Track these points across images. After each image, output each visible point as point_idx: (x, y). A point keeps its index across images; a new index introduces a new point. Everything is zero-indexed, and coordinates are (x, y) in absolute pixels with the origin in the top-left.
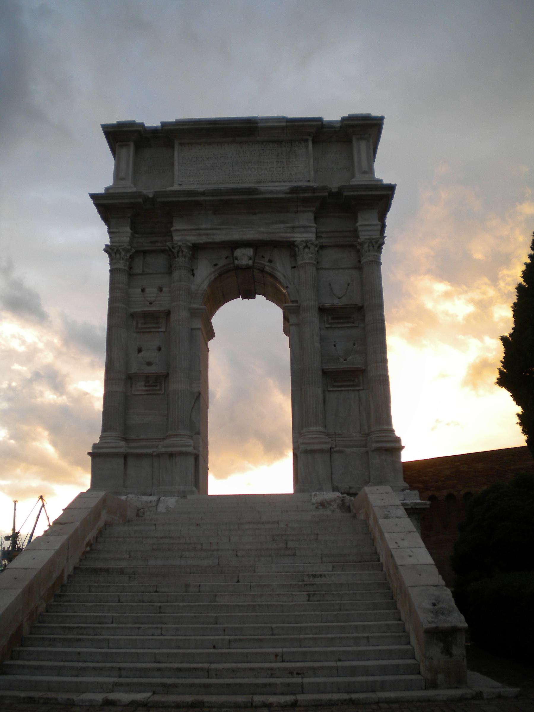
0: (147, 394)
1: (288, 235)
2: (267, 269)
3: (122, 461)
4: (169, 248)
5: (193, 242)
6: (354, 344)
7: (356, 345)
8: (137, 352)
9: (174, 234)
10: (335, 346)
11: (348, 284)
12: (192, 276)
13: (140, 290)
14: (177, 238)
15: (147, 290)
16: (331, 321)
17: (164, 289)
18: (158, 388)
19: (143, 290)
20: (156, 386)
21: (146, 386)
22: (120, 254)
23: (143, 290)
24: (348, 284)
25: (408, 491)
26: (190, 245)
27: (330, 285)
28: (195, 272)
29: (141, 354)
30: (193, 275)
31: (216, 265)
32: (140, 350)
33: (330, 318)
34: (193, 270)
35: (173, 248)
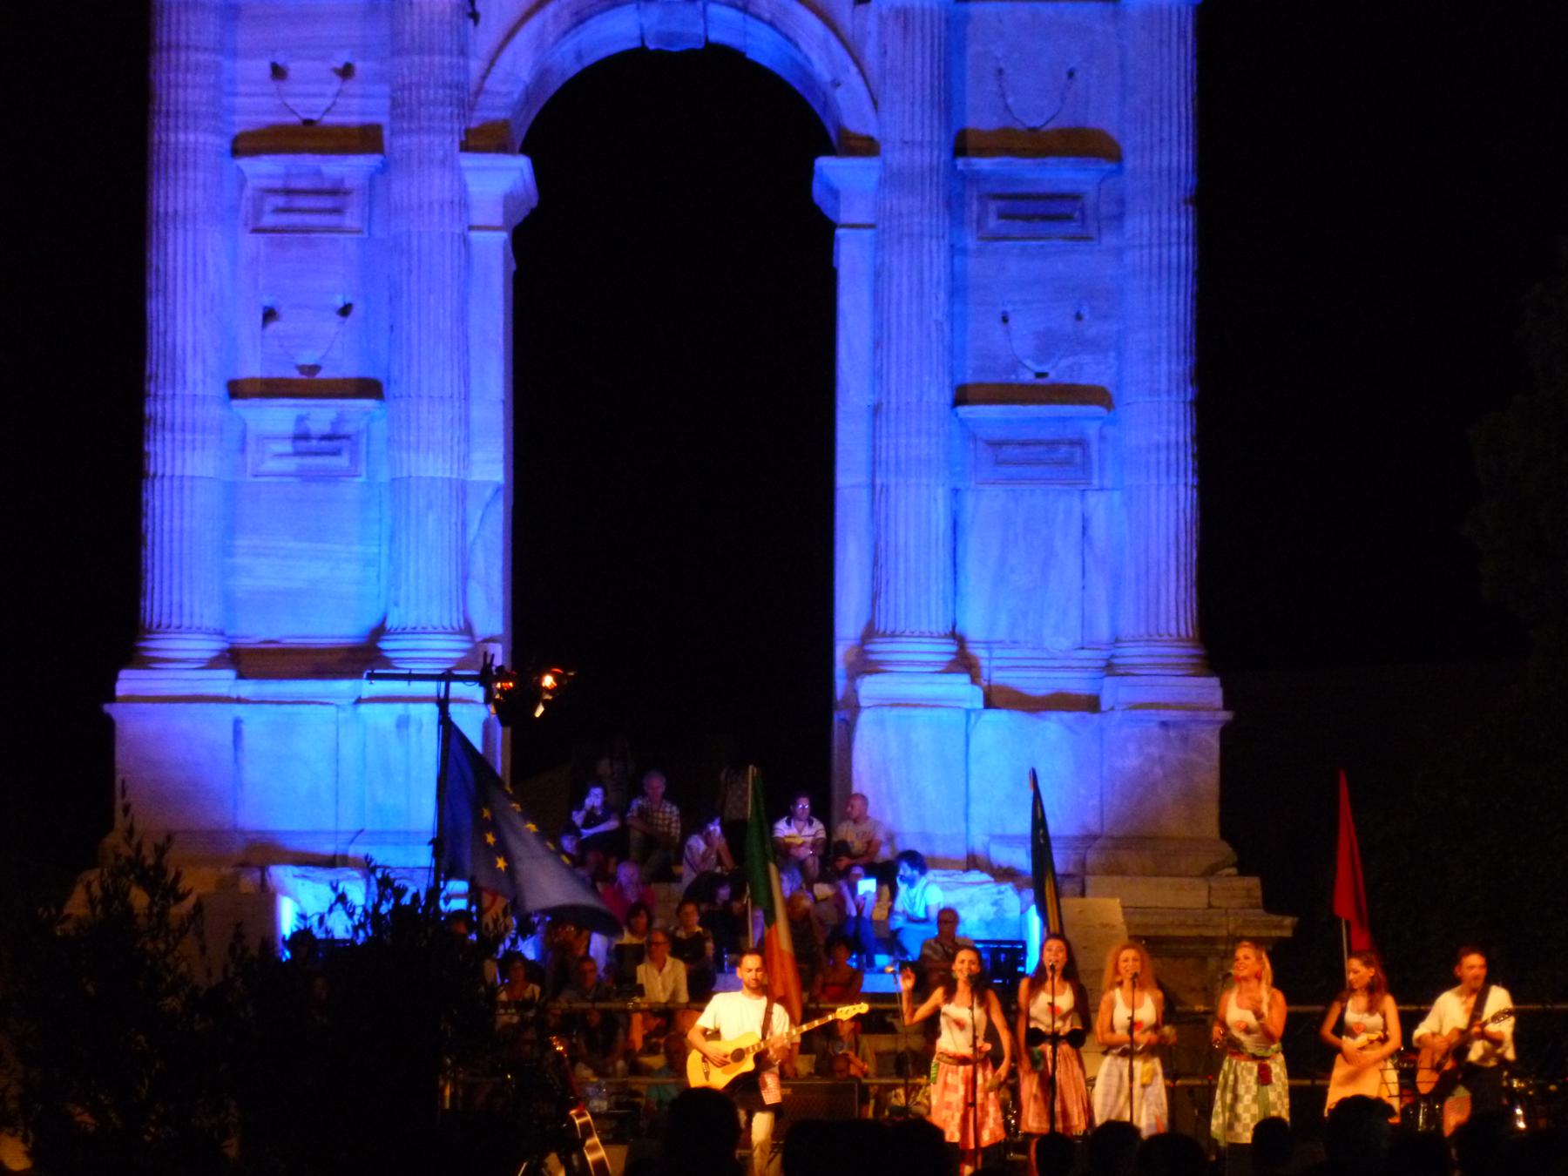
6: (1078, 317)
7: (1087, 317)
8: (260, 317)
10: (1005, 320)
11: (1071, 74)
12: (471, 22)
13: (265, 65)
15: (294, 67)
16: (993, 223)
18: (343, 461)
20: (336, 453)
21: (297, 453)
24: (1071, 74)
25: (1233, 871)
27: (1000, 71)
29: (274, 326)
30: (474, 16)
32: (269, 315)
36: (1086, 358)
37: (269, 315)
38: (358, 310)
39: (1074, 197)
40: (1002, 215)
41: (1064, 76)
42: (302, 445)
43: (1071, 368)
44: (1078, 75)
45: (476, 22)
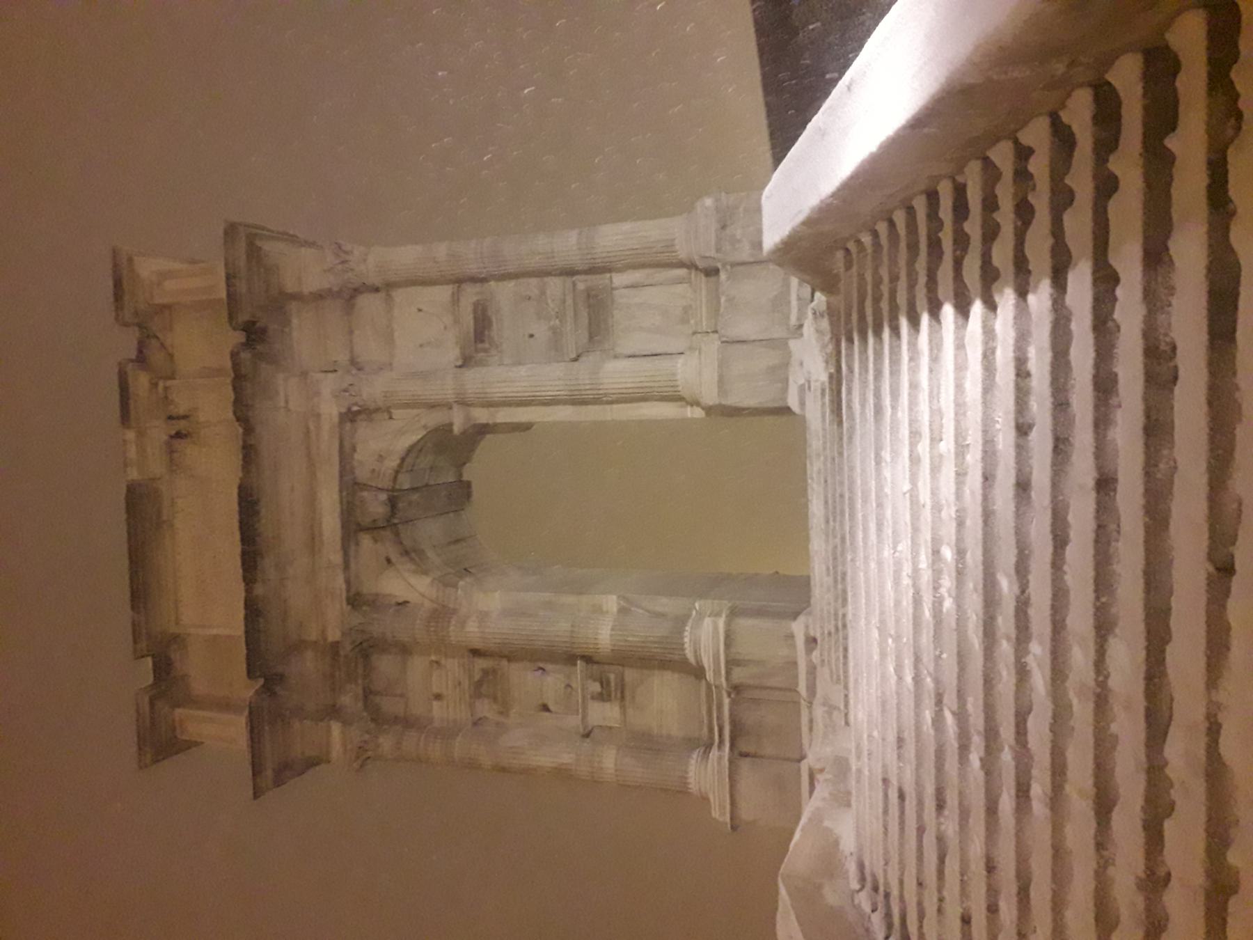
0: (623, 698)
1: (326, 427)
2: (392, 463)
3: (745, 764)
4: (353, 649)
5: (344, 603)
8: (547, 714)
9: (330, 639)
10: (531, 336)
11: (420, 310)
13: (435, 704)
14: (334, 635)
15: (435, 690)
16: (487, 345)
17: (433, 658)
18: (612, 677)
19: (438, 697)
22: (365, 742)
23: (438, 697)
24: (420, 310)
26: (349, 607)
28: (401, 600)
29: (551, 707)
31: (389, 561)
32: (545, 708)
33: (480, 346)
34: (399, 604)
35: (354, 642)
36: (548, 292)
37: (545, 708)
38: (541, 665)
39: (476, 305)
40: (482, 341)
41: (421, 314)
42: (605, 696)
43: (553, 300)
44: (421, 307)
45: (408, 602)
